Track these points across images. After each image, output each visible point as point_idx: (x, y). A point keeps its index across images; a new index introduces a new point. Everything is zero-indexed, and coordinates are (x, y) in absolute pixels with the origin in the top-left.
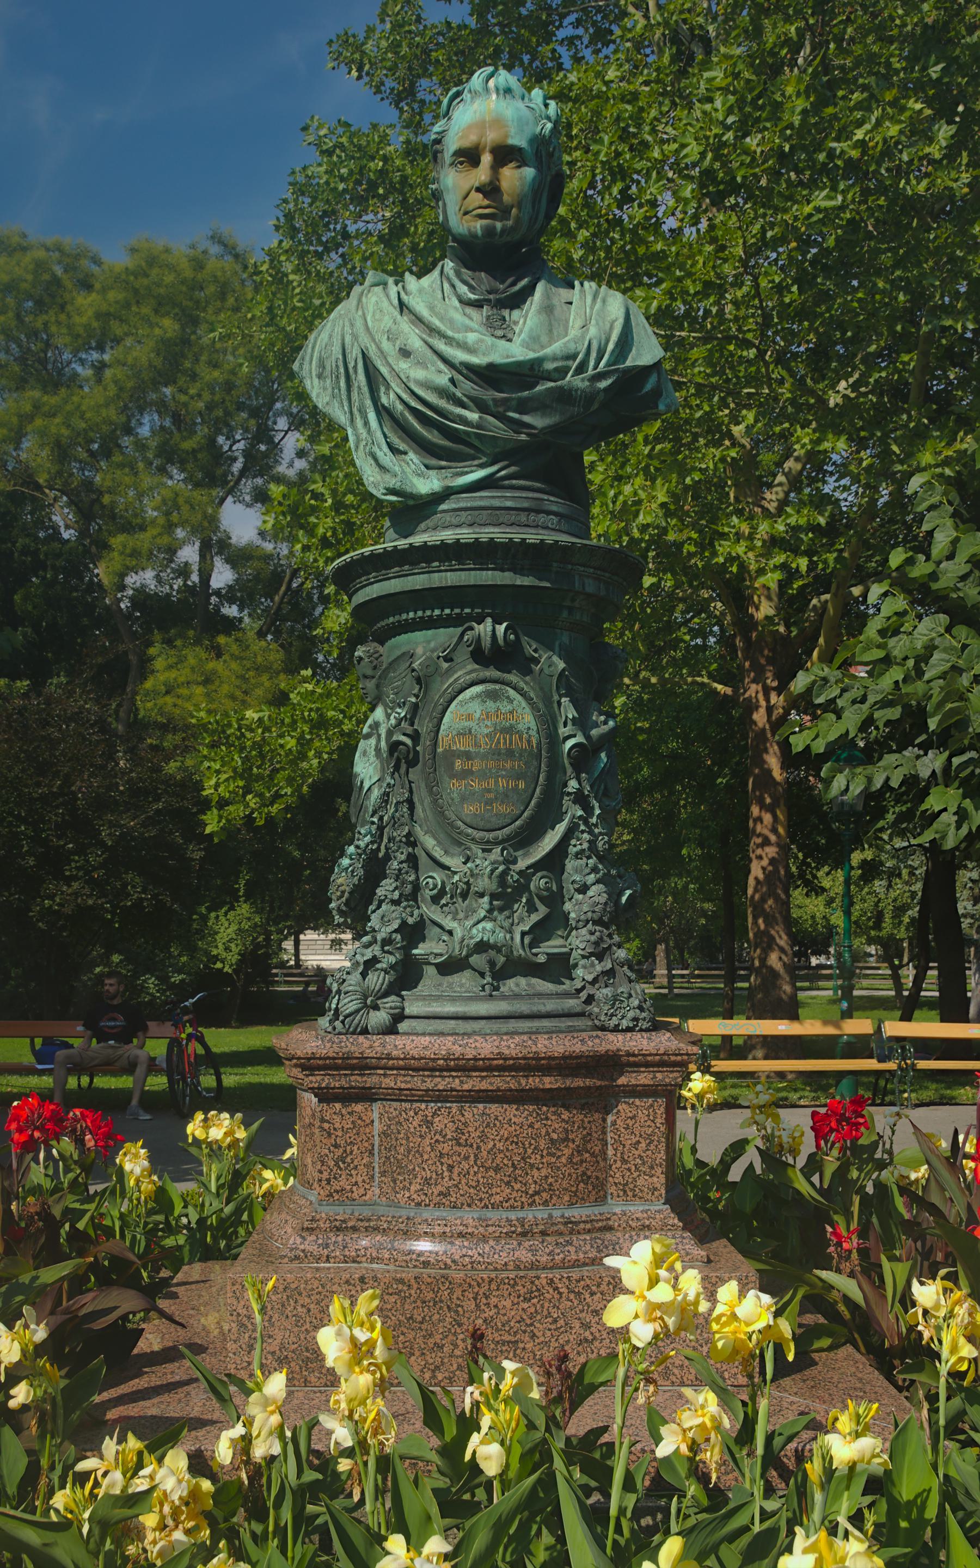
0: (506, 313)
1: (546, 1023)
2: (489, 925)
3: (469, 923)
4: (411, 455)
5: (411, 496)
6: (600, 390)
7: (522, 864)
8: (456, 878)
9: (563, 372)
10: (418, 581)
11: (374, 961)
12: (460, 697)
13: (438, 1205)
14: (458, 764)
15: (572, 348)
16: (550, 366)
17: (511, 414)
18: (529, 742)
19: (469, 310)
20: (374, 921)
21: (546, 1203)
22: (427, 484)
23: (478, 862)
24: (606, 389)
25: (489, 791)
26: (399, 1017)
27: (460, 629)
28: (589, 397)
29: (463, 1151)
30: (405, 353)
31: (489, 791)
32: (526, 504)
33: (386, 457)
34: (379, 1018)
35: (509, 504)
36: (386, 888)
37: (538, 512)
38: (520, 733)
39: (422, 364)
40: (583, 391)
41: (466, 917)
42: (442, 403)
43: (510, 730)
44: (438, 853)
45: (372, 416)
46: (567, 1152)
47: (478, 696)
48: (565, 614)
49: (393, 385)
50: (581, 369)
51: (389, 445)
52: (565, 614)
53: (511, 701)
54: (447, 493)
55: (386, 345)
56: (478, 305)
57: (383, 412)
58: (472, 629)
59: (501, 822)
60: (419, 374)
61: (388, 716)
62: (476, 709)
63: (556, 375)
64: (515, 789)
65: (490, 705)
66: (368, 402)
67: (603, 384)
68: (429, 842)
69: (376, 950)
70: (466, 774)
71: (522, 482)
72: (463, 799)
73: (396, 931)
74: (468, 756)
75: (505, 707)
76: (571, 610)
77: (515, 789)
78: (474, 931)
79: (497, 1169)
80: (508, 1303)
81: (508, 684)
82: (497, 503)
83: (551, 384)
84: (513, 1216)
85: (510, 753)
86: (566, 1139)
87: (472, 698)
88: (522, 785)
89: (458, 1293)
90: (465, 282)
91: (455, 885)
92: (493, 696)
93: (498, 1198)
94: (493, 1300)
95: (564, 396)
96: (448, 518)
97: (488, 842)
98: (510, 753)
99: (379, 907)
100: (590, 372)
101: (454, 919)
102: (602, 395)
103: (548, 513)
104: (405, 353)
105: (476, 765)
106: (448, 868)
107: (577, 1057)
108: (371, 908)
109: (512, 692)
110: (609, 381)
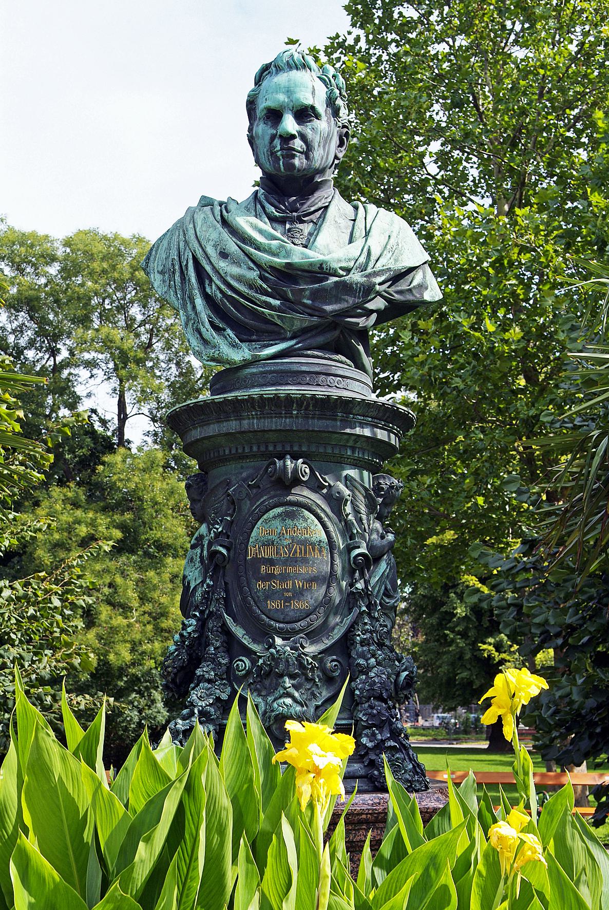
2: (288, 701)
3: (270, 699)
4: (229, 331)
5: (228, 362)
8: (261, 661)
10: (232, 426)
12: (265, 517)
14: (263, 569)
17: (305, 301)
19: (275, 225)
20: (194, 696)
22: (240, 354)
23: (278, 648)
25: (288, 591)
27: (266, 463)
30: (224, 255)
31: (288, 591)
33: (209, 333)
35: (304, 368)
36: (205, 670)
39: (237, 263)
41: (268, 695)
42: (252, 293)
44: (246, 641)
45: (199, 302)
47: (279, 515)
49: (214, 279)
51: (212, 324)
53: (306, 520)
54: (255, 361)
55: (210, 250)
56: (282, 221)
57: (207, 298)
58: (275, 463)
60: (235, 270)
61: (210, 530)
62: (277, 525)
63: (341, 272)
65: (289, 522)
66: (196, 292)
68: (239, 632)
70: (270, 577)
73: (211, 705)
74: (271, 562)
75: (301, 524)
78: (275, 705)
83: (336, 279)
87: (275, 517)
90: (272, 205)
91: (260, 668)
92: (291, 516)
97: (287, 632)
99: (197, 685)
101: (259, 695)
104: (224, 255)
105: (277, 571)
106: (255, 653)
107: (358, 814)
108: (192, 685)
109: (306, 513)
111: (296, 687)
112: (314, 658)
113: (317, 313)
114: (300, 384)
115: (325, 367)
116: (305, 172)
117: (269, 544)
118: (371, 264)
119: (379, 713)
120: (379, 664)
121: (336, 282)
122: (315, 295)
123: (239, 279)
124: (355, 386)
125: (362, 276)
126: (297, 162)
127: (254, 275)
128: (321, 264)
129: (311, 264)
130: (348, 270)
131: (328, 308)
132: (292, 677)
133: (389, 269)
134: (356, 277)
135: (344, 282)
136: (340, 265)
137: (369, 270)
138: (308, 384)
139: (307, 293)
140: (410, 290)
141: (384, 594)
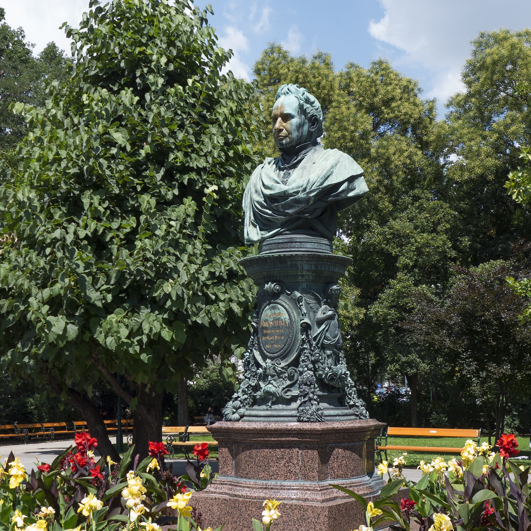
0: (291, 171)
1: (282, 419)
6: (311, 197)
7: (283, 364)
11: (239, 397)
13: (246, 477)
16: (291, 192)
18: (285, 323)
21: (276, 479)
24: (314, 196)
26: (242, 416)
29: (251, 460)
32: (286, 241)
34: (236, 416)
35: (280, 241)
38: (282, 320)
43: (278, 319)
46: (283, 462)
48: (300, 278)
50: (305, 190)
52: (300, 278)
53: (279, 309)
59: (276, 351)
62: (269, 312)
64: (281, 339)
65: (273, 311)
67: (312, 195)
69: (240, 394)
70: (266, 335)
72: (266, 343)
75: (277, 311)
76: (303, 276)
77: (281, 339)
79: (260, 467)
80: (254, 509)
81: (279, 304)
82: (276, 241)
84: (264, 482)
85: (279, 327)
86: (283, 458)
88: (283, 338)
89: (241, 505)
92: (274, 308)
93: (260, 476)
94: (250, 508)
95: (298, 201)
98: (279, 327)
100: (308, 191)
103: (296, 242)
110: (315, 193)
111: (275, 380)
112: (282, 368)
116: (290, 145)
117: (266, 321)
118: (308, 188)
119: (304, 390)
120: (308, 370)
123: (258, 202)
124: (309, 245)
127: (262, 200)
128: (285, 192)
129: (279, 193)
130: (297, 192)
131: (290, 211)
132: (273, 376)
134: (301, 195)
137: (308, 191)
140: (338, 195)
141: (324, 338)
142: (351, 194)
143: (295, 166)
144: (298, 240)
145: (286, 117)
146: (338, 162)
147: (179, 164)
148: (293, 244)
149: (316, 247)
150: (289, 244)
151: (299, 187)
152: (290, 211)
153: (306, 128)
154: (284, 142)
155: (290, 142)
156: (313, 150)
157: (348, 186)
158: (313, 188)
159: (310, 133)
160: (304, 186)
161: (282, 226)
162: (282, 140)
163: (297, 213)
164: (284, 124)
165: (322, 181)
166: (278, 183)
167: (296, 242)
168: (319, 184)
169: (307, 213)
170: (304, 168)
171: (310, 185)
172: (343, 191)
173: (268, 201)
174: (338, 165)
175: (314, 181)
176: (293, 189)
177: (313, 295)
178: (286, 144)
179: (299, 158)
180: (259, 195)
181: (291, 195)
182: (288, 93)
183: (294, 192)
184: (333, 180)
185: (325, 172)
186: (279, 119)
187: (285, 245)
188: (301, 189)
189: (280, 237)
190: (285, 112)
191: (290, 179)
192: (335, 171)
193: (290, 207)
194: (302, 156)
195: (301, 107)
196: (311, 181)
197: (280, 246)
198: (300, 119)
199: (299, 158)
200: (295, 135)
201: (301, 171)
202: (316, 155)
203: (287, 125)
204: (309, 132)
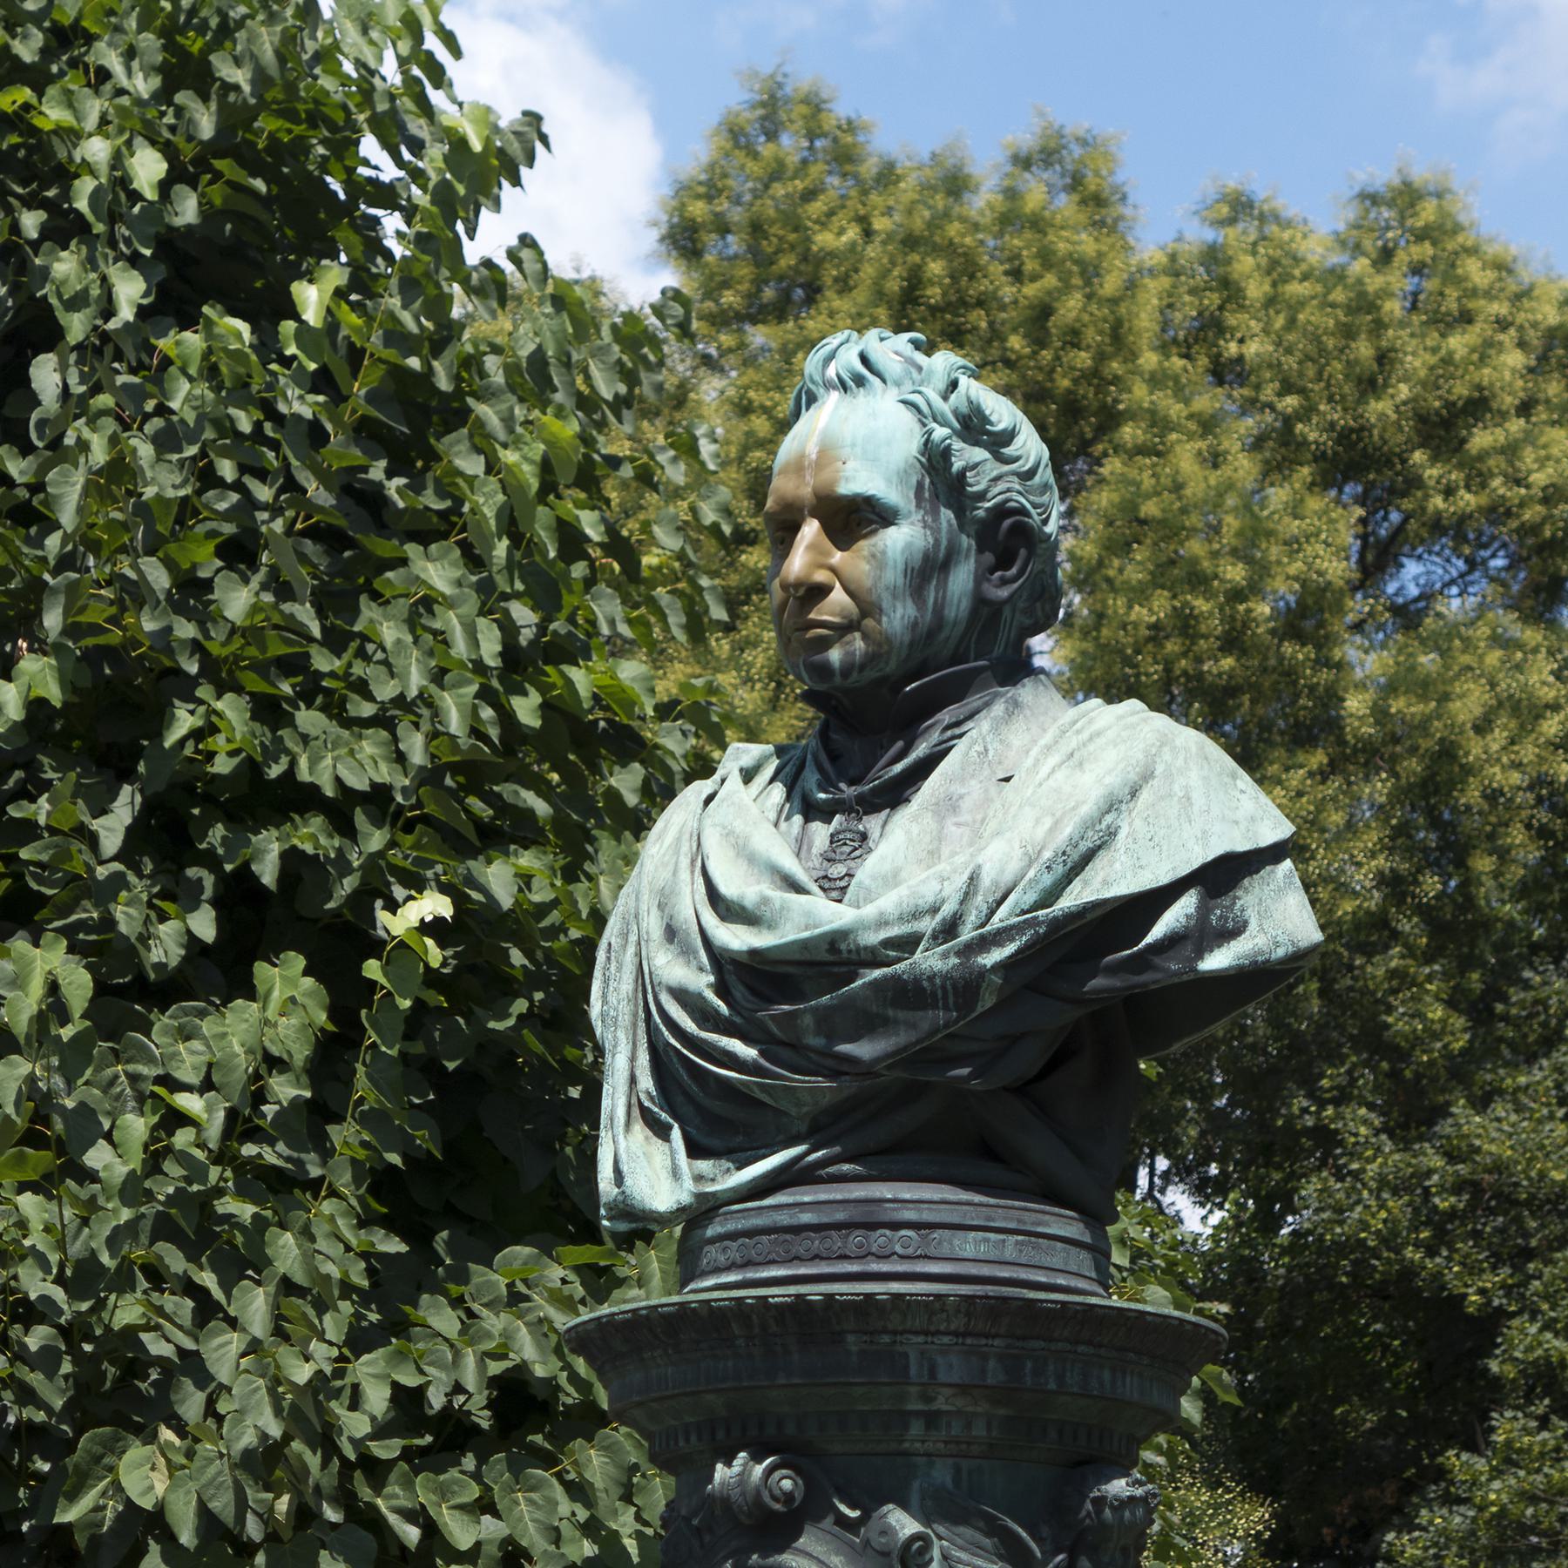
0: (872, 823)
6: (983, 973)
9: (908, 944)
15: (929, 894)
16: (872, 938)
24: (1000, 967)
28: (964, 987)
32: (840, 1216)
35: (806, 1218)
37: (872, 1226)
40: (946, 977)
48: (916, 1428)
50: (949, 929)
52: (916, 1428)
71: (846, 1167)
82: (784, 1219)
83: (877, 973)
95: (911, 994)
96: (734, 1251)
100: (967, 934)
102: (997, 980)
103: (896, 1226)
110: (1009, 949)
113: (845, 1068)
114: (798, 1259)
115: (867, 1208)
116: (871, 674)
118: (972, 918)
121: (875, 984)
122: (829, 1023)
123: (683, 996)
124: (969, 1245)
125: (945, 956)
126: (835, 655)
127: (701, 982)
128: (835, 940)
129: (804, 945)
131: (863, 1050)
133: (1033, 923)
134: (931, 960)
135: (896, 979)
136: (884, 934)
137: (967, 934)
138: (817, 1257)
139: (808, 1020)
142: (1217, 960)
143: (895, 795)
144: (909, 1215)
145: (852, 518)
146: (1147, 776)
147: (222, 765)
148: (880, 1238)
149: (1010, 1253)
150: (857, 1237)
151: (916, 915)
152: (863, 1050)
153: (961, 579)
154: (835, 655)
155: (871, 659)
156: (998, 708)
157: (1203, 910)
158: (996, 922)
159: (984, 611)
160: (947, 910)
161: (816, 1133)
162: (824, 644)
163: (903, 1059)
164: (837, 557)
165: (1047, 880)
166: (798, 888)
167: (896, 1226)
168: (1031, 898)
169: (958, 1061)
170: (948, 806)
171: (980, 902)
172: (1172, 941)
173: (739, 992)
174: (1145, 796)
175: (1007, 878)
176: (882, 923)
177: (994, 1529)
178: (847, 669)
179: (921, 750)
180: (686, 952)
181: (873, 958)
182: (860, 381)
183: (888, 943)
184: (1112, 879)
185: (1068, 830)
186: (811, 529)
187: (836, 1241)
188: (927, 925)
189: (806, 1195)
190: (845, 489)
191: (869, 869)
192: (1130, 826)
193: (864, 1022)
194: (935, 736)
195: (935, 460)
196: (986, 880)
197: (802, 1245)
198: (931, 526)
199: (921, 750)
200: (898, 617)
201: (928, 820)
202: (1018, 734)
203: (854, 561)
204: (980, 601)
